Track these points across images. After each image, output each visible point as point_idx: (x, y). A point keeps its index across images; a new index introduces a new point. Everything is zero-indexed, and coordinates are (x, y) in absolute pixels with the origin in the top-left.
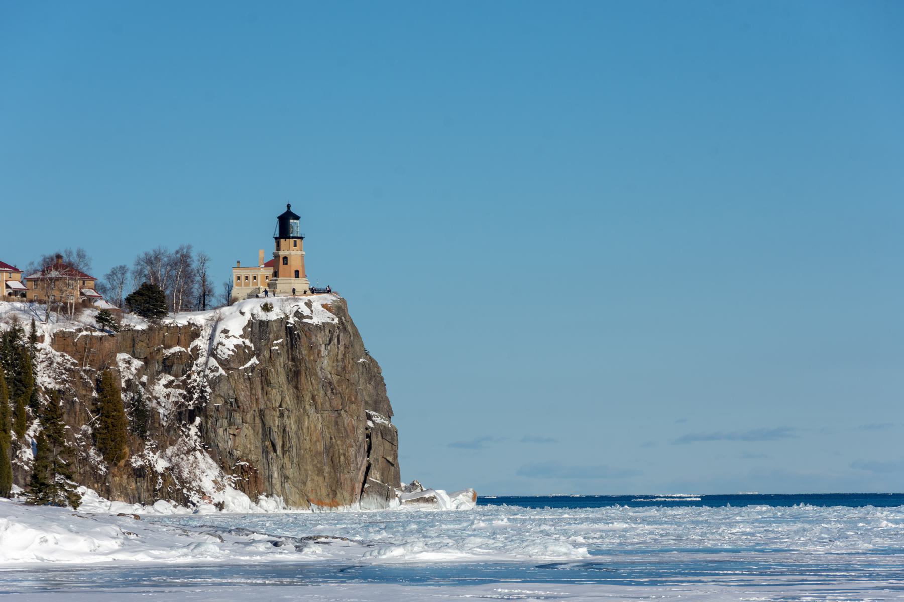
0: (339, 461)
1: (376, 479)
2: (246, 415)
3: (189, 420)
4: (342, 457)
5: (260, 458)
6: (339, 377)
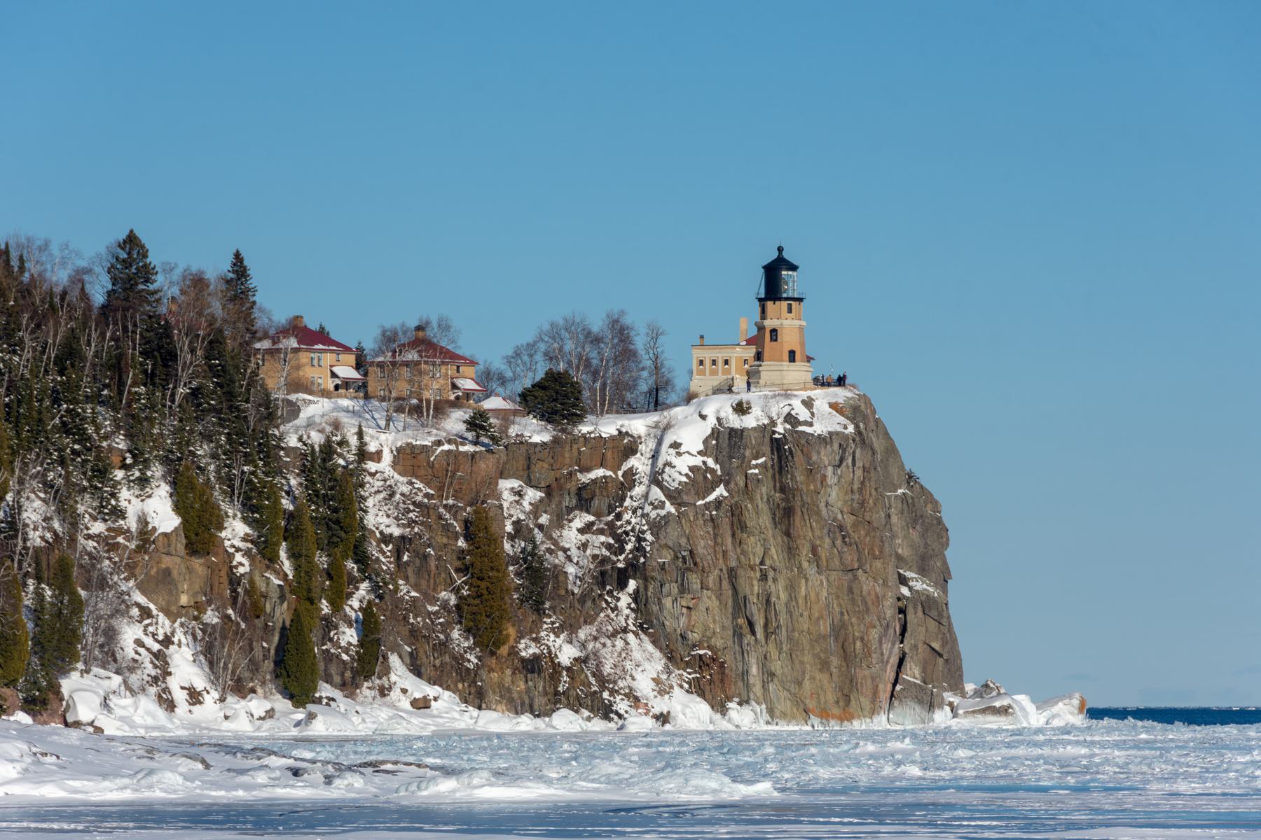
0: (854, 649)
1: (914, 677)
2: (708, 576)
3: (619, 584)
4: (858, 644)
5: (730, 643)
6: (854, 517)
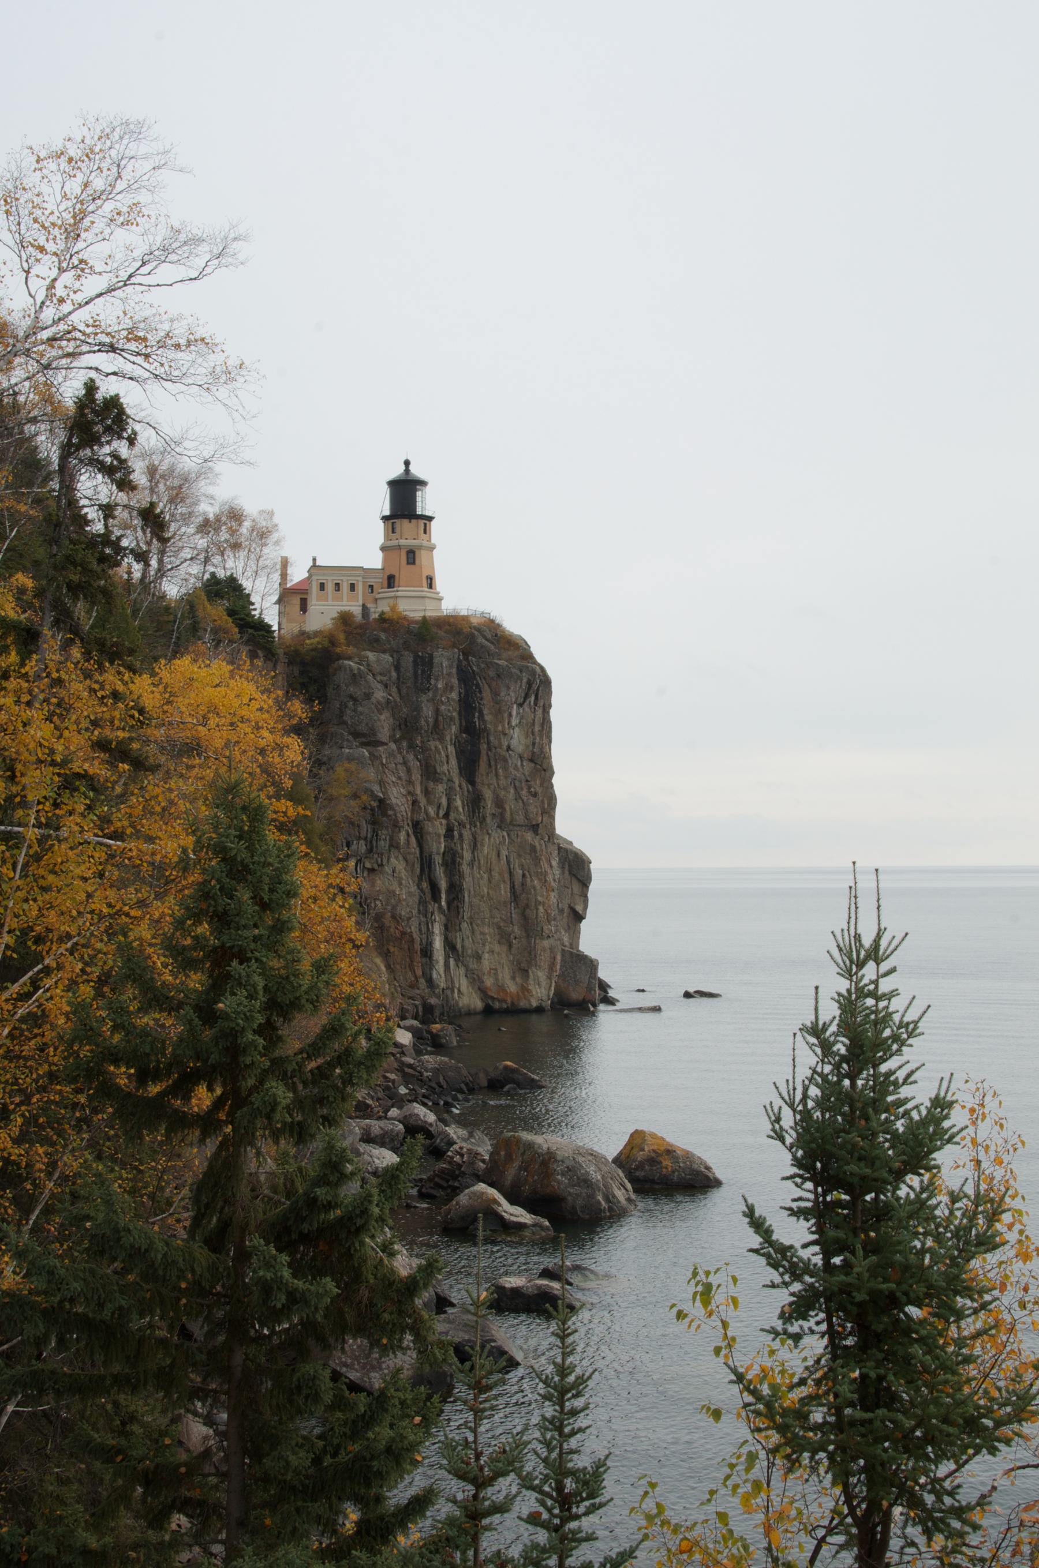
4: (541, 909)
5: (415, 912)
